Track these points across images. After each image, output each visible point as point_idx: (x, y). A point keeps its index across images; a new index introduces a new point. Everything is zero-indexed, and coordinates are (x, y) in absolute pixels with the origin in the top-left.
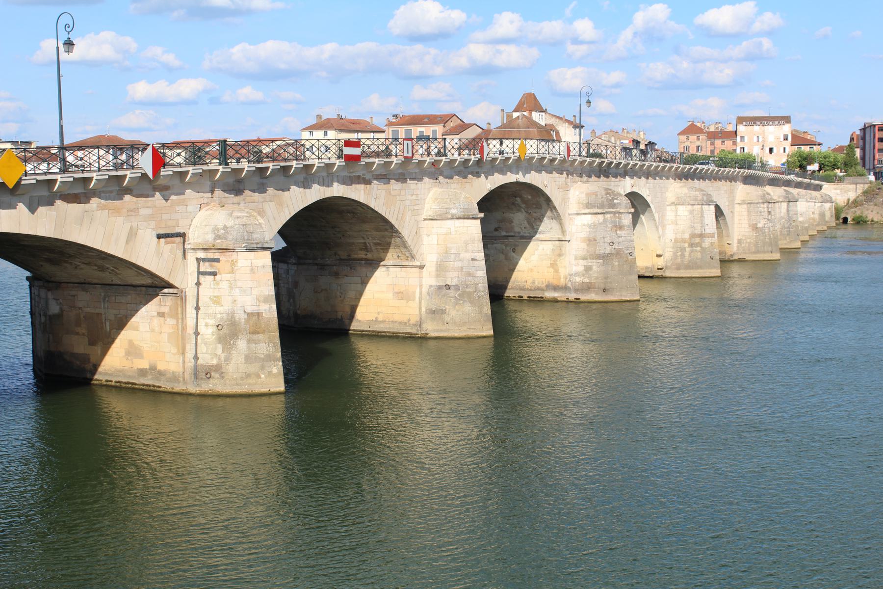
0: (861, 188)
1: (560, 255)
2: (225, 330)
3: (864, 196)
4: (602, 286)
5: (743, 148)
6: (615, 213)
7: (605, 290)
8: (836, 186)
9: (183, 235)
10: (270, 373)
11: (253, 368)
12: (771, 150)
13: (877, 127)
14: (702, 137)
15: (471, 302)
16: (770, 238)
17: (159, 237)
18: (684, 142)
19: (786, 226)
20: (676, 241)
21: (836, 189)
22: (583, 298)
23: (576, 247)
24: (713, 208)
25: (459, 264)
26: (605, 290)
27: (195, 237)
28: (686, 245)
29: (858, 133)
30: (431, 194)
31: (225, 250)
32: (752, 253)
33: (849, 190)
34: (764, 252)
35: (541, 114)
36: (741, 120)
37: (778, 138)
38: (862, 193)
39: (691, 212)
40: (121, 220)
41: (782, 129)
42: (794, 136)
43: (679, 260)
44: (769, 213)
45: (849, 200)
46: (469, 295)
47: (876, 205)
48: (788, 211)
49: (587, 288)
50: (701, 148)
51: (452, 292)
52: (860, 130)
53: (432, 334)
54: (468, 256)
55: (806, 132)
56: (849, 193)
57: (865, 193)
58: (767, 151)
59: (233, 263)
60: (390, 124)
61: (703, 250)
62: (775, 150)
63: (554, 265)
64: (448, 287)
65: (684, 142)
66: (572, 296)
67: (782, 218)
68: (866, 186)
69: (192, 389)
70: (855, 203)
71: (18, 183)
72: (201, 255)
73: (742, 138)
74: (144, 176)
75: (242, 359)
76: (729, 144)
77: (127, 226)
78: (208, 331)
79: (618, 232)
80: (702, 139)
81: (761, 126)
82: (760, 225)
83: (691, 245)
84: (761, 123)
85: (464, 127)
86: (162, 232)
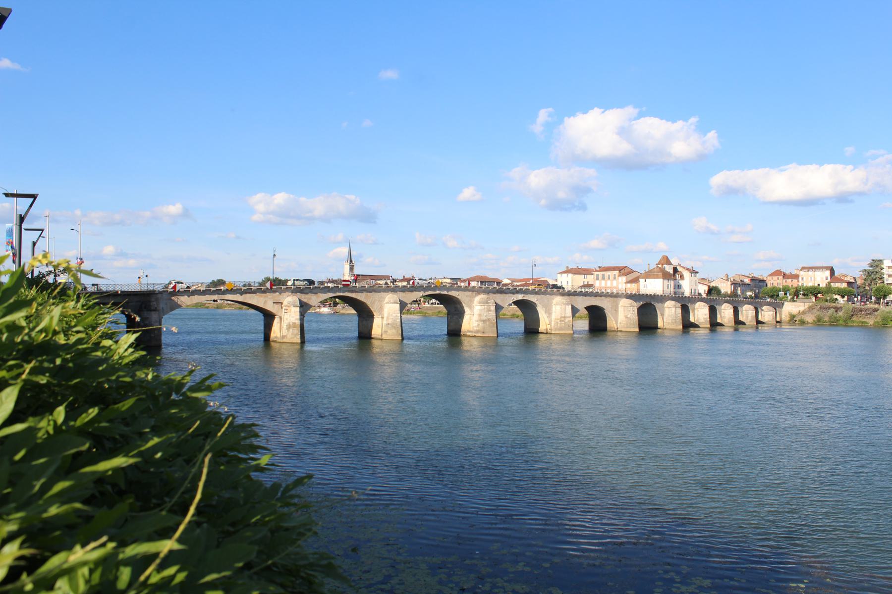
0: (807, 305)
1: (471, 320)
2: (288, 327)
4: (483, 331)
6: (488, 305)
7: (483, 332)
8: (791, 304)
9: (282, 303)
10: (297, 338)
11: (293, 336)
14: (781, 278)
15: (395, 329)
16: (633, 322)
17: (274, 303)
19: (674, 318)
20: (555, 319)
21: (792, 305)
22: (477, 335)
23: (476, 317)
24: (570, 307)
25: (392, 317)
26: (483, 332)
27: (285, 303)
28: (559, 321)
30: (388, 296)
31: (289, 307)
32: (624, 328)
33: (800, 306)
34: (631, 328)
35: (670, 266)
36: (803, 268)
37: (822, 279)
39: (561, 308)
40: (262, 298)
43: (556, 327)
44: (633, 311)
45: (800, 311)
46: (394, 327)
47: (812, 314)
48: (675, 312)
49: (477, 331)
51: (390, 326)
53: (384, 338)
54: (396, 315)
56: (800, 307)
57: (809, 307)
59: (291, 310)
60: (596, 271)
61: (565, 323)
63: (469, 324)
64: (388, 324)
66: (474, 334)
67: (672, 315)
68: (811, 304)
69: (281, 341)
70: (804, 313)
71: (232, 289)
72: (285, 308)
73: (802, 279)
74: (268, 288)
75: (290, 334)
76: (795, 281)
77: (264, 300)
78: (285, 327)
79: (489, 312)
82: (629, 316)
83: (561, 321)
85: (632, 272)
86: (275, 302)
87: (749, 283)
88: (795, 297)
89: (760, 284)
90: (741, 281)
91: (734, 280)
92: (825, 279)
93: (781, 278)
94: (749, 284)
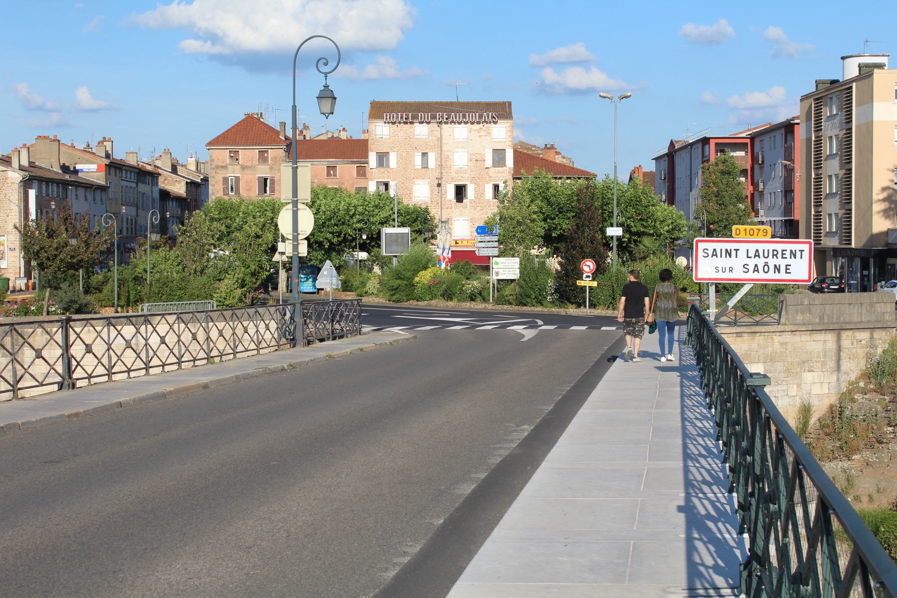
3: (880, 390)
5: (387, 185)
12: (460, 192)
13: (712, 142)
18: (225, 167)
29: (650, 167)
33: (806, 364)
36: (379, 110)
38: (867, 375)
41: (489, 133)
42: (518, 155)
50: (273, 183)
52: (656, 159)
55: (552, 147)
56: (808, 377)
62: (470, 192)
65: (225, 167)
73: (382, 158)
76: (346, 171)
80: (274, 159)
81: (434, 126)
84: (434, 117)
87: (103, 183)
88: (588, 266)
89: (143, 188)
90: (65, 169)
91: (32, 165)
92: (489, 162)
93: (276, 153)
94: (103, 189)
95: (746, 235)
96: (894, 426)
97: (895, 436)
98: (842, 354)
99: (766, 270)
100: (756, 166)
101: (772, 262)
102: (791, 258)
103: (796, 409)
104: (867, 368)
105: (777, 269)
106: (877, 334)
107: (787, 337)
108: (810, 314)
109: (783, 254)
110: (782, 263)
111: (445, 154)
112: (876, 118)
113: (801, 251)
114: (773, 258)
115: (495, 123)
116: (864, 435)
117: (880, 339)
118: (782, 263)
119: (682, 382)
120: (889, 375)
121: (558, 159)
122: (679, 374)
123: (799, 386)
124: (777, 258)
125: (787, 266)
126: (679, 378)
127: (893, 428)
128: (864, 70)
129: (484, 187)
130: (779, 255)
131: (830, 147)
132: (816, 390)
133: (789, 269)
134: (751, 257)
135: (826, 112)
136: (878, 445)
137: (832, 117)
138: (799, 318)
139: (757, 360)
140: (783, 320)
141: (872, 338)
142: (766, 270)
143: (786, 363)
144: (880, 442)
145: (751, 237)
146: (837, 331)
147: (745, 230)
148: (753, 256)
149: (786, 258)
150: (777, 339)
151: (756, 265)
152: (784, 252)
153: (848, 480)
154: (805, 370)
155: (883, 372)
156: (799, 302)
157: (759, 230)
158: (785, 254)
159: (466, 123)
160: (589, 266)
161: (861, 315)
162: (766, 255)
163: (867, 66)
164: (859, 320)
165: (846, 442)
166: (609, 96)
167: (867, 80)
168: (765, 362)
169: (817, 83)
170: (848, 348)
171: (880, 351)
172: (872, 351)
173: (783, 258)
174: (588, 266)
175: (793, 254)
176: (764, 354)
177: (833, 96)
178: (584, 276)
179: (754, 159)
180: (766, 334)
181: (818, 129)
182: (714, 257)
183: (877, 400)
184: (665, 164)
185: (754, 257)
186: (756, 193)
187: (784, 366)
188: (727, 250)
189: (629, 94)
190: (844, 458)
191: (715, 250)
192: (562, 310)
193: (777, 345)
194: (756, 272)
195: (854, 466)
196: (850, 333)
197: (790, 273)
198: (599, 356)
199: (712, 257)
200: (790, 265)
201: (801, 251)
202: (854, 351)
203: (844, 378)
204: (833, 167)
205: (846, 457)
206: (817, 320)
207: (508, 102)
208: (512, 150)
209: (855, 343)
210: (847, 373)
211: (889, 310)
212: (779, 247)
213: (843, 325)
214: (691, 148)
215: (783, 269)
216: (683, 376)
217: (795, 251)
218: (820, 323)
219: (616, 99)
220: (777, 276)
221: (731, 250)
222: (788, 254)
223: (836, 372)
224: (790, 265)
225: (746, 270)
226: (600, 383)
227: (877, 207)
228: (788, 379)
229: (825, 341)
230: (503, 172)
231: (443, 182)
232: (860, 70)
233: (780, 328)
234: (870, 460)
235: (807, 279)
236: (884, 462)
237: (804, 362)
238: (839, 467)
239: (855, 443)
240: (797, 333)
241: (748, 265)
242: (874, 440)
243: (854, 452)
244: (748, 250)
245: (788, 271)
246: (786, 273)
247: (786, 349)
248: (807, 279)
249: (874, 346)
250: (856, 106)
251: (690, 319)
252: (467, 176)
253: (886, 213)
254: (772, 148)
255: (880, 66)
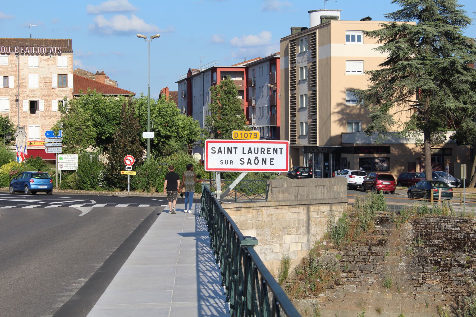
3: (337, 246)
12: (33, 106)
13: (219, 71)
29: (174, 88)
33: (285, 229)
37: (48, 82)
38: (329, 237)
41: (55, 63)
42: (77, 79)
47: (386, 285)
52: (179, 82)
55: (102, 73)
56: (287, 239)
58: (26, 107)
62: (41, 106)
81: (13, 56)
84: (13, 50)
88: (129, 160)
92: (55, 84)
95: (242, 137)
96: (347, 273)
97: (348, 279)
98: (310, 222)
99: (256, 162)
100: (250, 88)
101: (260, 156)
102: (274, 154)
103: (279, 262)
104: (328, 231)
105: (264, 161)
106: (334, 208)
107: (272, 211)
108: (288, 193)
109: (268, 151)
110: (268, 157)
111: (22, 77)
112: (332, 55)
113: (281, 149)
114: (261, 153)
115: (60, 55)
116: (327, 279)
117: (337, 211)
118: (268, 157)
119: (197, 244)
120: (343, 236)
121: (107, 82)
122: (195, 238)
123: (281, 245)
124: (264, 153)
125: (271, 159)
126: (195, 241)
127: (346, 274)
128: (324, 21)
129: (51, 102)
130: (266, 152)
131: (301, 75)
132: (293, 248)
133: (272, 162)
134: (246, 153)
135: (298, 50)
136: (336, 286)
137: (302, 53)
138: (281, 196)
139: (251, 227)
140: (269, 198)
141: (331, 210)
142: (256, 162)
143: (272, 229)
144: (338, 284)
145: (245, 139)
146: (307, 206)
147: (242, 134)
148: (247, 153)
149: (270, 154)
150: (265, 211)
151: (249, 159)
152: (269, 150)
153: (316, 312)
154: (285, 234)
155: (339, 234)
156: (281, 185)
157: (252, 134)
158: (270, 151)
159: (37, 55)
160: (130, 160)
161: (324, 194)
162: (256, 152)
163: (326, 18)
164: (322, 197)
165: (314, 285)
166: (144, 36)
167: (326, 28)
168: (257, 229)
169: (292, 29)
170: (315, 218)
171: (337, 219)
172: (332, 219)
173: (268, 153)
174: (129, 160)
175: (275, 151)
176: (256, 222)
177: (303, 39)
178: (126, 167)
179: (248, 83)
180: (258, 208)
181: (293, 62)
182: (220, 153)
183: (335, 254)
184: (184, 87)
185: (248, 153)
186: (250, 107)
187: (270, 231)
188: (228, 148)
189: (158, 35)
190: (313, 296)
191: (220, 148)
192: (110, 192)
193: (265, 216)
194: (249, 164)
195: (320, 302)
196: (316, 207)
197: (273, 164)
198: (137, 226)
199: (218, 153)
200: (273, 159)
201: (281, 149)
202: (319, 219)
203: (312, 240)
204: (303, 89)
205: (314, 295)
206: (293, 198)
207: (69, 40)
208: (73, 75)
209: (320, 214)
210: (314, 236)
211: (343, 190)
212: (266, 146)
213: (311, 201)
214: (204, 75)
215: (268, 162)
216: (198, 240)
217: (277, 148)
218: (295, 200)
219: (149, 39)
220: (264, 167)
221: (231, 148)
222: (271, 151)
223: (307, 235)
224: (273, 159)
225: (242, 163)
226: (138, 246)
227: (334, 118)
228: (273, 240)
229: (299, 213)
230: (65, 91)
231: (20, 99)
232: (321, 20)
233: (267, 204)
234: (331, 297)
235: (285, 168)
236: (340, 298)
237: (284, 228)
238: (309, 303)
239: (321, 285)
240: (279, 207)
241: (243, 159)
242: (333, 283)
243: (320, 291)
244: (243, 148)
245: (272, 163)
246: (271, 164)
247: (272, 219)
248: (285, 168)
249: (332, 216)
250: (319, 46)
251: (203, 198)
252: (38, 93)
253: (341, 122)
254: (261, 75)
255: (335, 18)
